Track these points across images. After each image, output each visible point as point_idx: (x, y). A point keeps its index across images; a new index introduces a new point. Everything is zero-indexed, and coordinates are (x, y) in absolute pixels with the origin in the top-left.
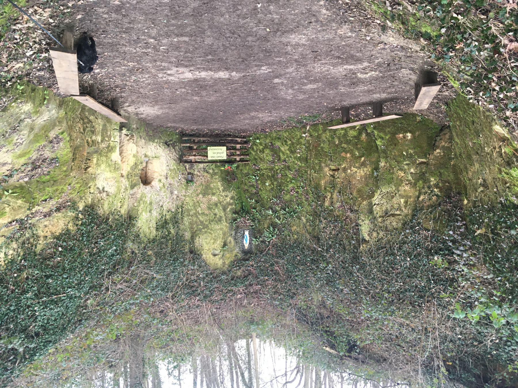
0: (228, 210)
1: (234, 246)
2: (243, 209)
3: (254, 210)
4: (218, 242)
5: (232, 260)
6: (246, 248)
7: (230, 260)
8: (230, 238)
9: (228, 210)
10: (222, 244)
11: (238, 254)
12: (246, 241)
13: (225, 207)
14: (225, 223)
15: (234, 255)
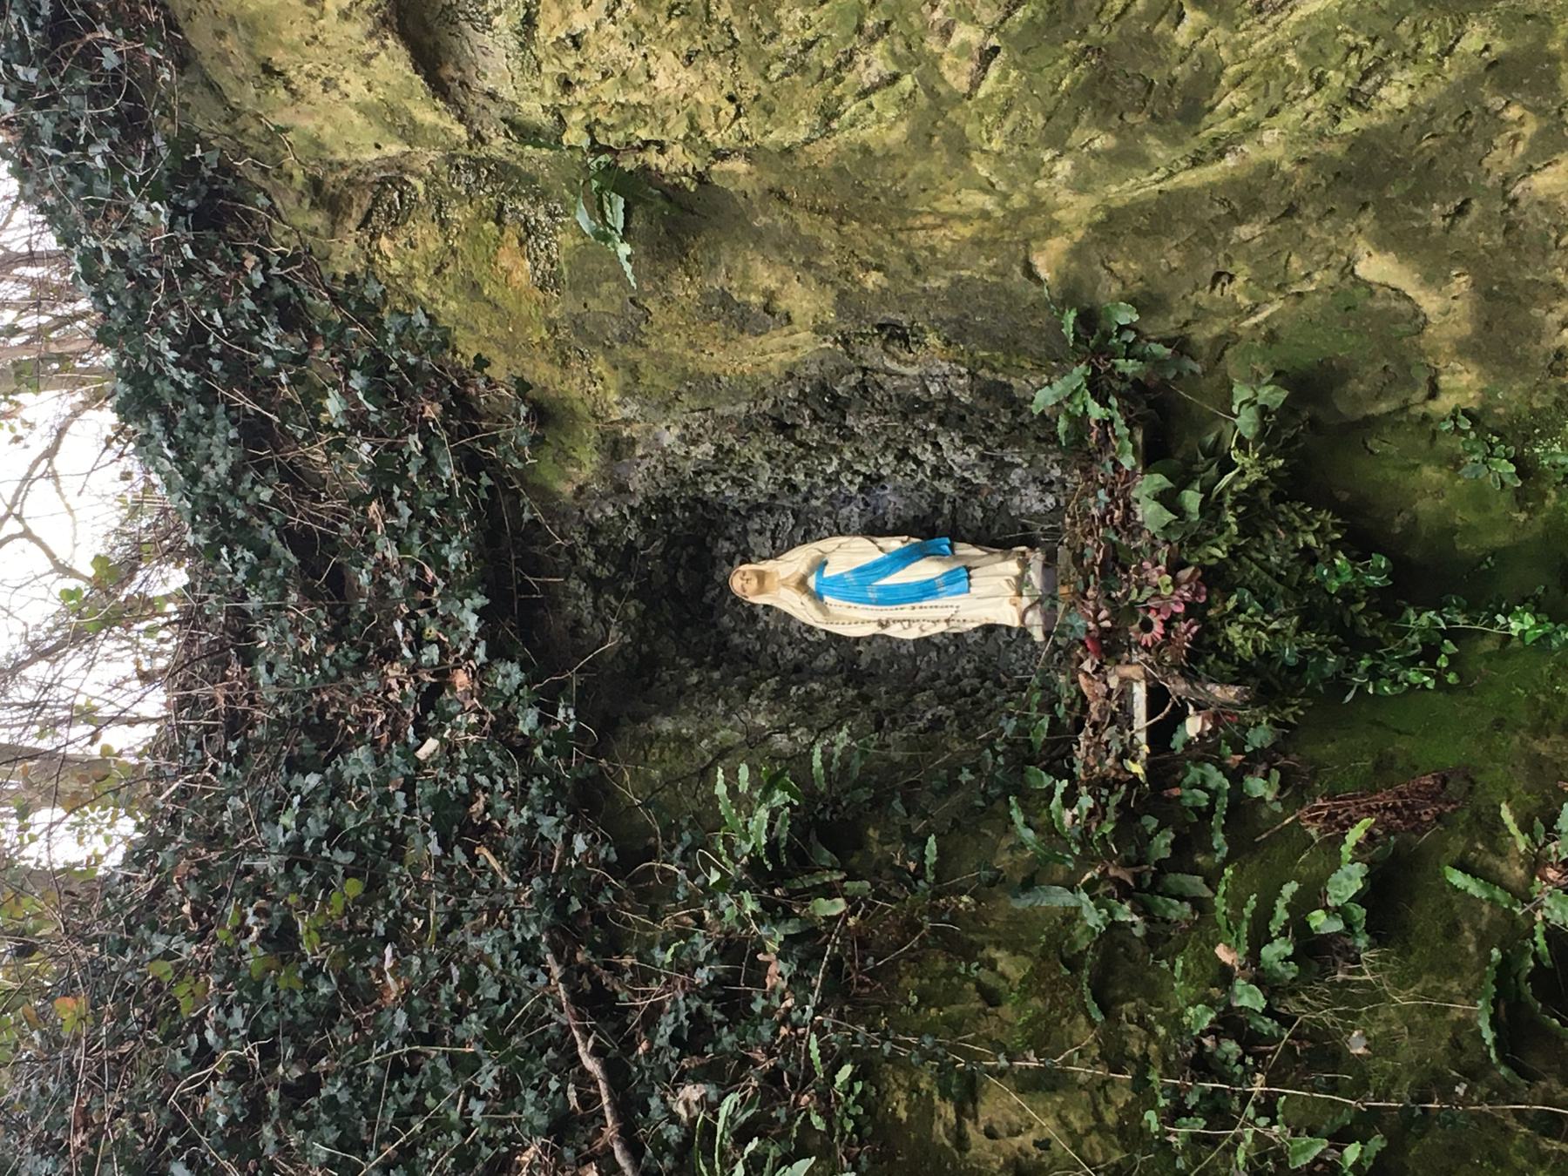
0: (1376, 267)
1: (706, 385)
2: (1388, 603)
3: (1348, 881)
4: (670, 77)
5: (468, 348)
6: (742, 581)
7: (451, 308)
8: (803, 300)
9: (1376, 267)
10: (675, 161)
11: (587, 465)
12: (860, 584)
13: (1426, 183)
14: (1075, 210)
15: (542, 373)
